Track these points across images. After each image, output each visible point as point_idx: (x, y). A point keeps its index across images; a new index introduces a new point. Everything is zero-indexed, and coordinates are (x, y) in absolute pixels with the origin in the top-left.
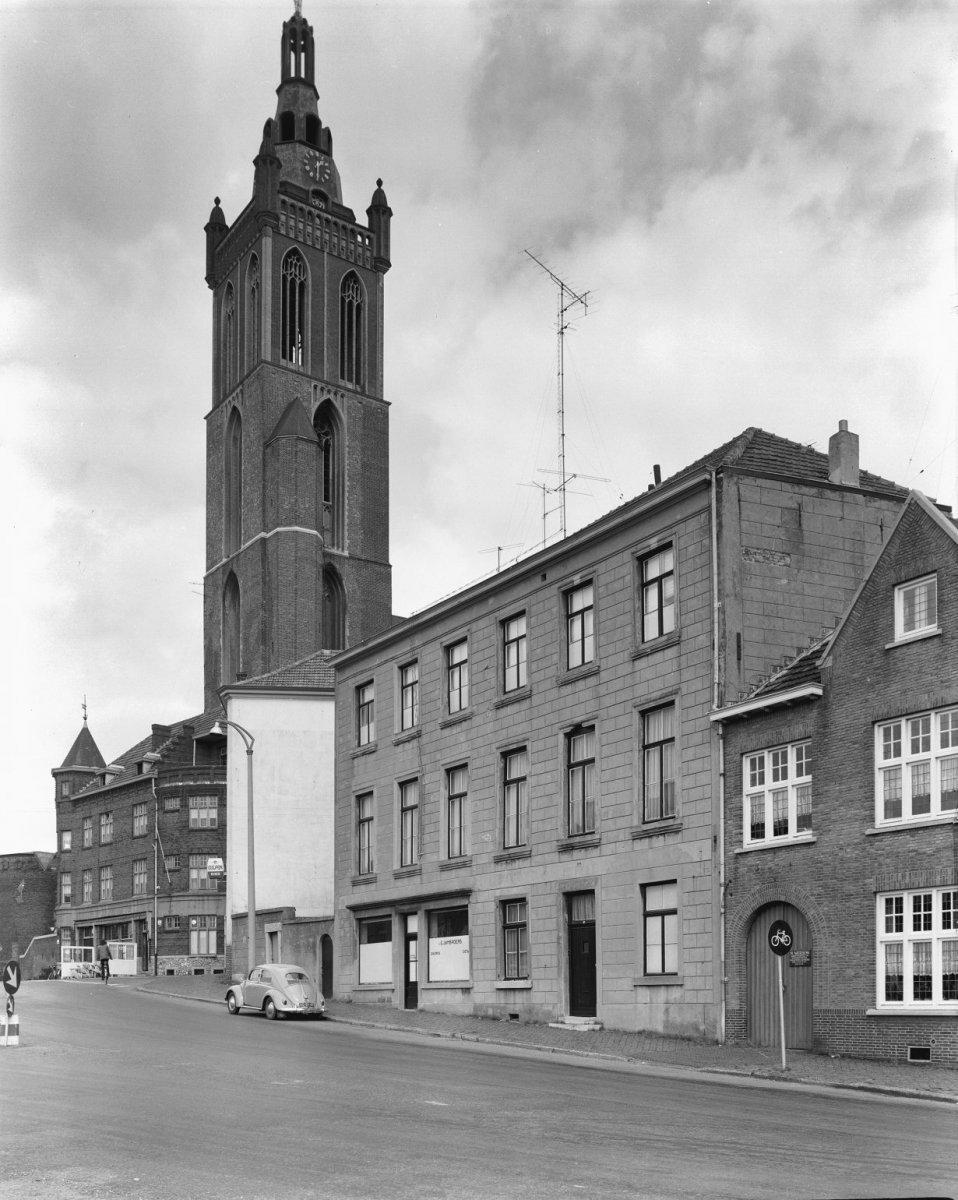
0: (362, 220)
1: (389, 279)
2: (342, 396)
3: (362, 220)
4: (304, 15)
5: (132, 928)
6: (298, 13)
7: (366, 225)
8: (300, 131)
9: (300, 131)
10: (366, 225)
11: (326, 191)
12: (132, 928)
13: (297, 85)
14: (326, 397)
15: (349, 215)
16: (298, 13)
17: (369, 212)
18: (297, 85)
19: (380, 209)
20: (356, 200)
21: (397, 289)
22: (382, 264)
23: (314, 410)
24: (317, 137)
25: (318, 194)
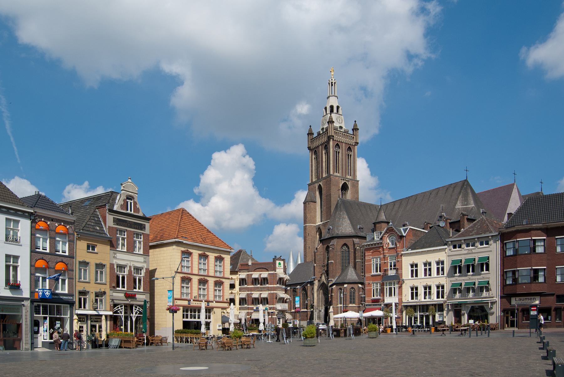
2: (349, 181)
7: (352, 134)
14: (344, 181)
23: (341, 186)
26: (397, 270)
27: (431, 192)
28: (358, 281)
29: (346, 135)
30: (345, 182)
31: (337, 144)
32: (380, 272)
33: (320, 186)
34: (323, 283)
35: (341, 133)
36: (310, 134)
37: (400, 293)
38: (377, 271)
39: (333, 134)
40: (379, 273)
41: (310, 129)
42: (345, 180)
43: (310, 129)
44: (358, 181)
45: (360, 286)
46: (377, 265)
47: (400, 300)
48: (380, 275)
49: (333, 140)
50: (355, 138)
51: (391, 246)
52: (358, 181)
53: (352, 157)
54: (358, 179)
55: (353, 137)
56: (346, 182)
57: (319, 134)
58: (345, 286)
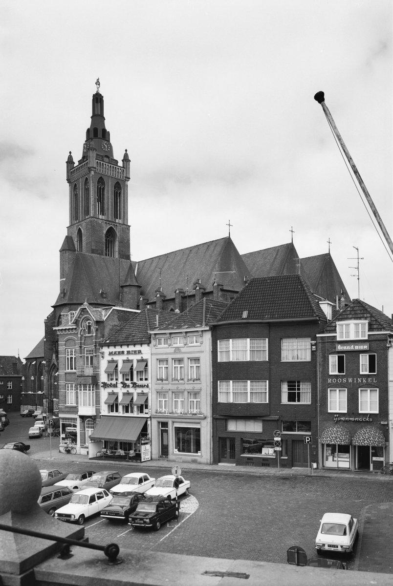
0: (120, 164)
1: (129, 183)
3: (120, 164)
5: (74, 327)
7: (122, 166)
8: (100, 134)
9: (100, 134)
10: (122, 166)
11: (107, 155)
15: (117, 162)
17: (123, 161)
19: (126, 159)
20: (118, 156)
23: (105, 232)
24: (105, 135)
25: (107, 157)
27: (191, 249)
29: (113, 167)
30: (111, 227)
32: (75, 369)
33: (80, 230)
35: (105, 165)
36: (70, 161)
38: (72, 369)
39: (95, 166)
40: (74, 370)
42: (111, 224)
46: (71, 358)
47: (98, 411)
48: (75, 373)
49: (95, 172)
50: (125, 171)
54: (129, 224)
55: (123, 170)
56: (113, 227)
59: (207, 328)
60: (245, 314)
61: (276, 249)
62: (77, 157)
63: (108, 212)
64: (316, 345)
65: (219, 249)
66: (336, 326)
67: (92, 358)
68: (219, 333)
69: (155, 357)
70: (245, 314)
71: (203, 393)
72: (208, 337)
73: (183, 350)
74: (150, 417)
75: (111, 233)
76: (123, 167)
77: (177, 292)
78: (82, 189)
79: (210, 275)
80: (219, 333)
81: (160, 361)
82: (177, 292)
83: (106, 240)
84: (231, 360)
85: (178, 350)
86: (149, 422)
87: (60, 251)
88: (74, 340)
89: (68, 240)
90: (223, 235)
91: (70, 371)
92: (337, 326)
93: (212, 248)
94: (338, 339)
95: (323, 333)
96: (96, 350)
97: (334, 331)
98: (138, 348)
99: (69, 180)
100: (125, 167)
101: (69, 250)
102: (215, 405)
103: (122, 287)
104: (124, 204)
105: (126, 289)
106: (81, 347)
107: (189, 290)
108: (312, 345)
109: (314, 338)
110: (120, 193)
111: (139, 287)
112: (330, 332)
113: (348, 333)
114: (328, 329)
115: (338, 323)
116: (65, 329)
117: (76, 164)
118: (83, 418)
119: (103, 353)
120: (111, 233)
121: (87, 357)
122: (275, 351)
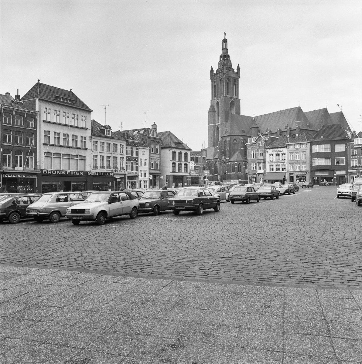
0: (236, 71)
1: (240, 79)
3: (236, 71)
4: (226, 38)
5: (256, 143)
6: (225, 38)
7: (236, 72)
8: (227, 57)
10: (236, 72)
12: (256, 143)
13: (225, 49)
15: (234, 69)
16: (225, 38)
18: (225, 49)
19: (238, 69)
20: (234, 67)
21: (242, 82)
22: (239, 77)
23: (230, 103)
26: (264, 157)
28: (242, 160)
31: (228, 78)
34: (223, 161)
36: (212, 71)
37: (265, 168)
38: (254, 157)
40: (254, 158)
41: (212, 69)
43: (212, 69)
44: (240, 99)
45: (244, 163)
46: (254, 154)
47: (265, 171)
51: (260, 145)
52: (240, 99)
53: (237, 85)
54: (240, 98)
57: (217, 71)
58: (236, 163)
59: (309, 142)
60: (322, 137)
61: (319, 111)
62: (215, 69)
63: (231, 93)
64: (347, 146)
65: (295, 112)
66: (354, 140)
67: (262, 153)
68: (312, 144)
69: (289, 152)
70: (322, 137)
71: (307, 163)
72: (309, 145)
73: (299, 149)
74: (287, 172)
75: (232, 103)
76: (237, 72)
77: (278, 130)
78: (219, 83)
79: (293, 123)
80: (312, 144)
81: (291, 153)
82: (278, 130)
83: (231, 107)
84: (318, 152)
85: (297, 149)
86: (286, 174)
87: (208, 112)
88: (255, 147)
89: (212, 106)
90: (297, 106)
91: (253, 158)
92: (354, 140)
93: (292, 111)
94: (355, 144)
95: (349, 142)
96: (264, 150)
97: (353, 141)
98: (282, 149)
99: (211, 79)
100: (238, 72)
101: (213, 111)
102: (311, 166)
103: (251, 128)
104: (238, 91)
105: (252, 129)
106: (258, 150)
107: (283, 129)
108: (346, 146)
109: (347, 144)
110: (236, 84)
111: (258, 128)
112: (352, 142)
113: (358, 142)
114: (351, 141)
115: (354, 139)
116: (251, 144)
117: (215, 72)
118: (259, 174)
119: (267, 151)
120: (232, 103)
121: (260, 153)
122: (333, 149)
